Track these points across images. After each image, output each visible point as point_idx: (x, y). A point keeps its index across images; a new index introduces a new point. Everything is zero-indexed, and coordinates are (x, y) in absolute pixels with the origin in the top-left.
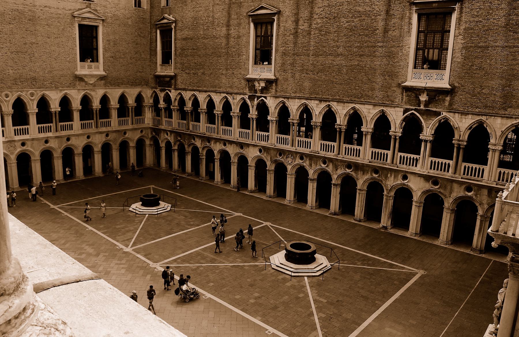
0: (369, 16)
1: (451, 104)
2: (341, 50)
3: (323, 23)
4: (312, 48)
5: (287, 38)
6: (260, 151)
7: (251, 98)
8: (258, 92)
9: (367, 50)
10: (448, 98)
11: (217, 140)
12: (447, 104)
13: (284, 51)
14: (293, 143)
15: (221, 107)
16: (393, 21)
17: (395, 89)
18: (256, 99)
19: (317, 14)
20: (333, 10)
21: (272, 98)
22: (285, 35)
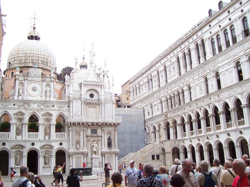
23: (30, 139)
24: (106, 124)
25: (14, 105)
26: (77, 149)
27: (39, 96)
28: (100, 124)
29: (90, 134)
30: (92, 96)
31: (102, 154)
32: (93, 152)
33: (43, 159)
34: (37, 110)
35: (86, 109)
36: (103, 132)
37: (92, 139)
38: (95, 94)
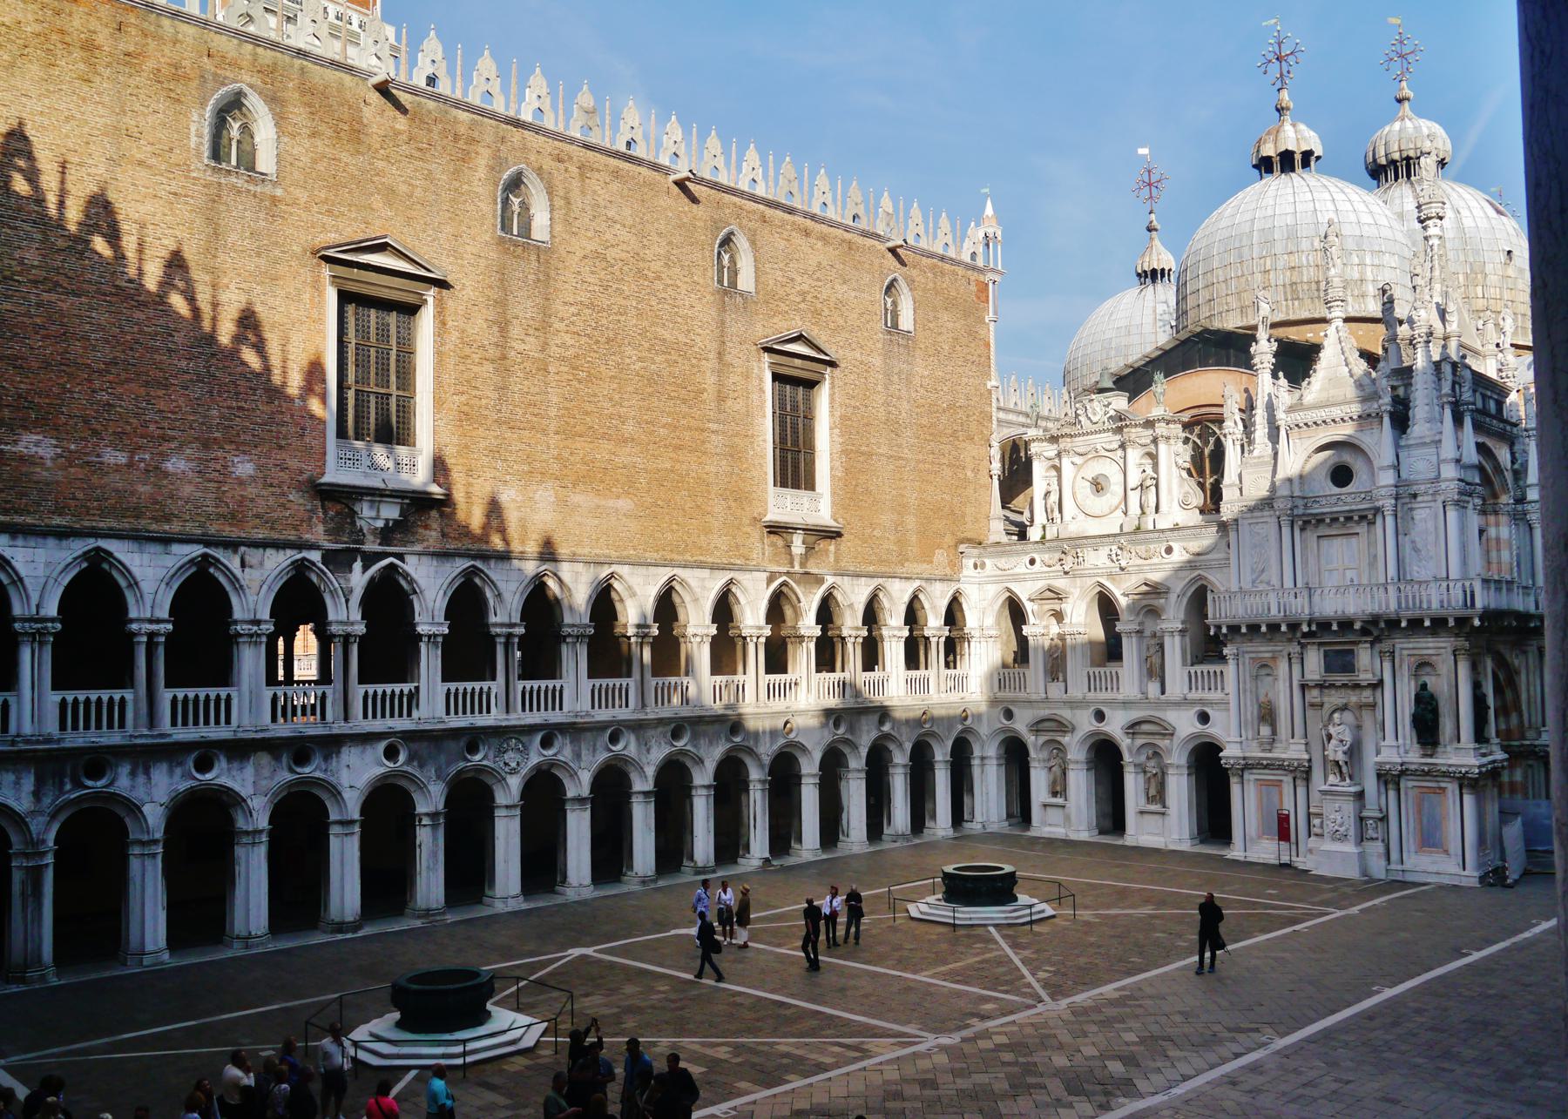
0: (685, 356)
1: (837, 560)
2: (629, 428)
3: (580, 347)
4: (553, 412)
5: (476, 369)
6: (391, 753)
7: (339, 560)
8: (370, 537)
9: (687, 435)
10: (832, 548)
11: (145, 756)
12: (832, 558)
13: (465, 408)
14: (501, 701)
15: (167, 607)
16: (734, 378)
17: (748, 529)
18: (358, 565)
19: (562, 320)
20: (604, 321)
21: (425, 559)
22: (467, 357)
23: (1091, 695)
24: (1393, 624)
25: (1032, 562)
26: (1261, 744)
27: (1119, 513)
28: (1357, 626)
29: (1317, 677)
30: (1341, 475)
31: (1379, 776)
32: (1329, 766)
33: (1141, 777)
34: (1110, 575)
35: (1304, 549)
36: (1387, 666)
37: (1334, 699)
38: (1357, 465)
